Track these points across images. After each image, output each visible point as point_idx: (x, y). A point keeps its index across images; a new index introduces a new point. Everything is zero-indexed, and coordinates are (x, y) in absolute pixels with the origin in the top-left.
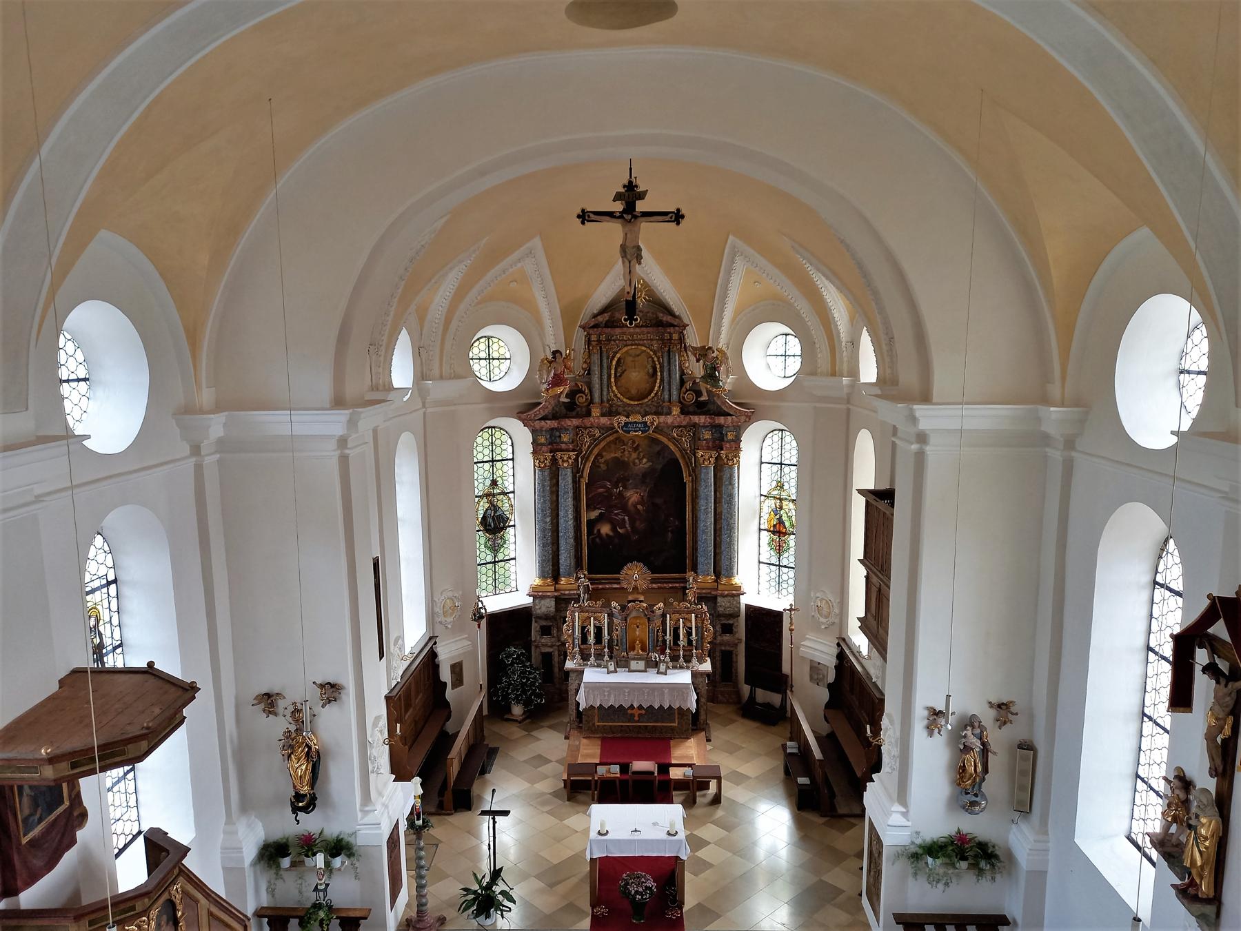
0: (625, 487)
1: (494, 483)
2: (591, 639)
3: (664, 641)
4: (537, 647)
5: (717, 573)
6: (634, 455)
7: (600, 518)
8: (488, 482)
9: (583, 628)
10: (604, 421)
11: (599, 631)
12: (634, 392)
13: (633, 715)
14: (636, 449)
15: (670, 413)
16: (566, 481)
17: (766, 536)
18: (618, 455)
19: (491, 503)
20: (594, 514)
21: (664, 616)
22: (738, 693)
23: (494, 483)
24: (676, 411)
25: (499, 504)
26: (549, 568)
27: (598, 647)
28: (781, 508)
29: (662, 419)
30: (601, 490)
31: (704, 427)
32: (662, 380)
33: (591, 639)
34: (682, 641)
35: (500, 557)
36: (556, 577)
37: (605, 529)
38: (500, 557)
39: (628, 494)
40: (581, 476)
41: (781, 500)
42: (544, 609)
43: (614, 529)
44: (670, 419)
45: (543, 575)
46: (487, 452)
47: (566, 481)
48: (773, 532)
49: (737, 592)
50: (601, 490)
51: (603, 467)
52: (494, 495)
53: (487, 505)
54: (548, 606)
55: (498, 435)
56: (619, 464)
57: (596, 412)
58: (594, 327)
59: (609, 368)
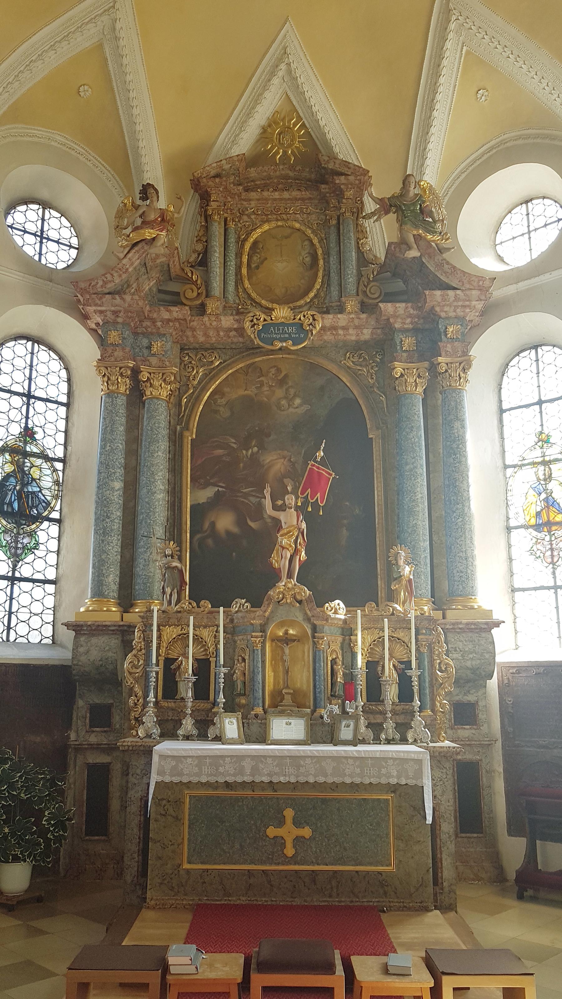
0: (261, 447)
1: (28, 433)
2: (187, 692)
3: (350, 678)
4: (78, 749)
5: (439, 601)
6: (280, 393)
7: (216, 502)
8: (16, 429)
9: (169, 661)
10: (228, 321)
11: (203, 667)
12: (279, 291)
13: (279, 842)
14: (282, 382)
15: (341, 310)
16: (159, 420)
17: (523, 540)
18: (251, 391)
19: (20, 467)
20: (206, 495)
21: (347, 631)
22: (496, 858)
23: (28, 433)
24: (351, 305)
25: (35, 473)
26: (112, 579)
27: (203, 705)
28: (549, 478)
29: (329, 320)
30: (220, 452)
31: (405, 331)
32: (327, 274)
33: (187, 692)
34: (391, 693)
35: (25, 571)
36: (126, 602)
37: (225, 522)
38: (25, 571)
39: (268, 458)
40: (187, 428)
41: (545, 463)
42: (95, 655)
43: (241, 522)
44: (342, 319)
45: (98, 592)
46: (19, 376)
47: (159, 420)
48: (537, 527)
49: (485, 626)
50: (220, 452)
51: (225, 413)
52: (26, 455)
53: (9, 468)
54: (99, 649)
55: (43, 354)
56: (251, 406)
57: (211, 306)
58: (217, 176)
59: (239, 255)
